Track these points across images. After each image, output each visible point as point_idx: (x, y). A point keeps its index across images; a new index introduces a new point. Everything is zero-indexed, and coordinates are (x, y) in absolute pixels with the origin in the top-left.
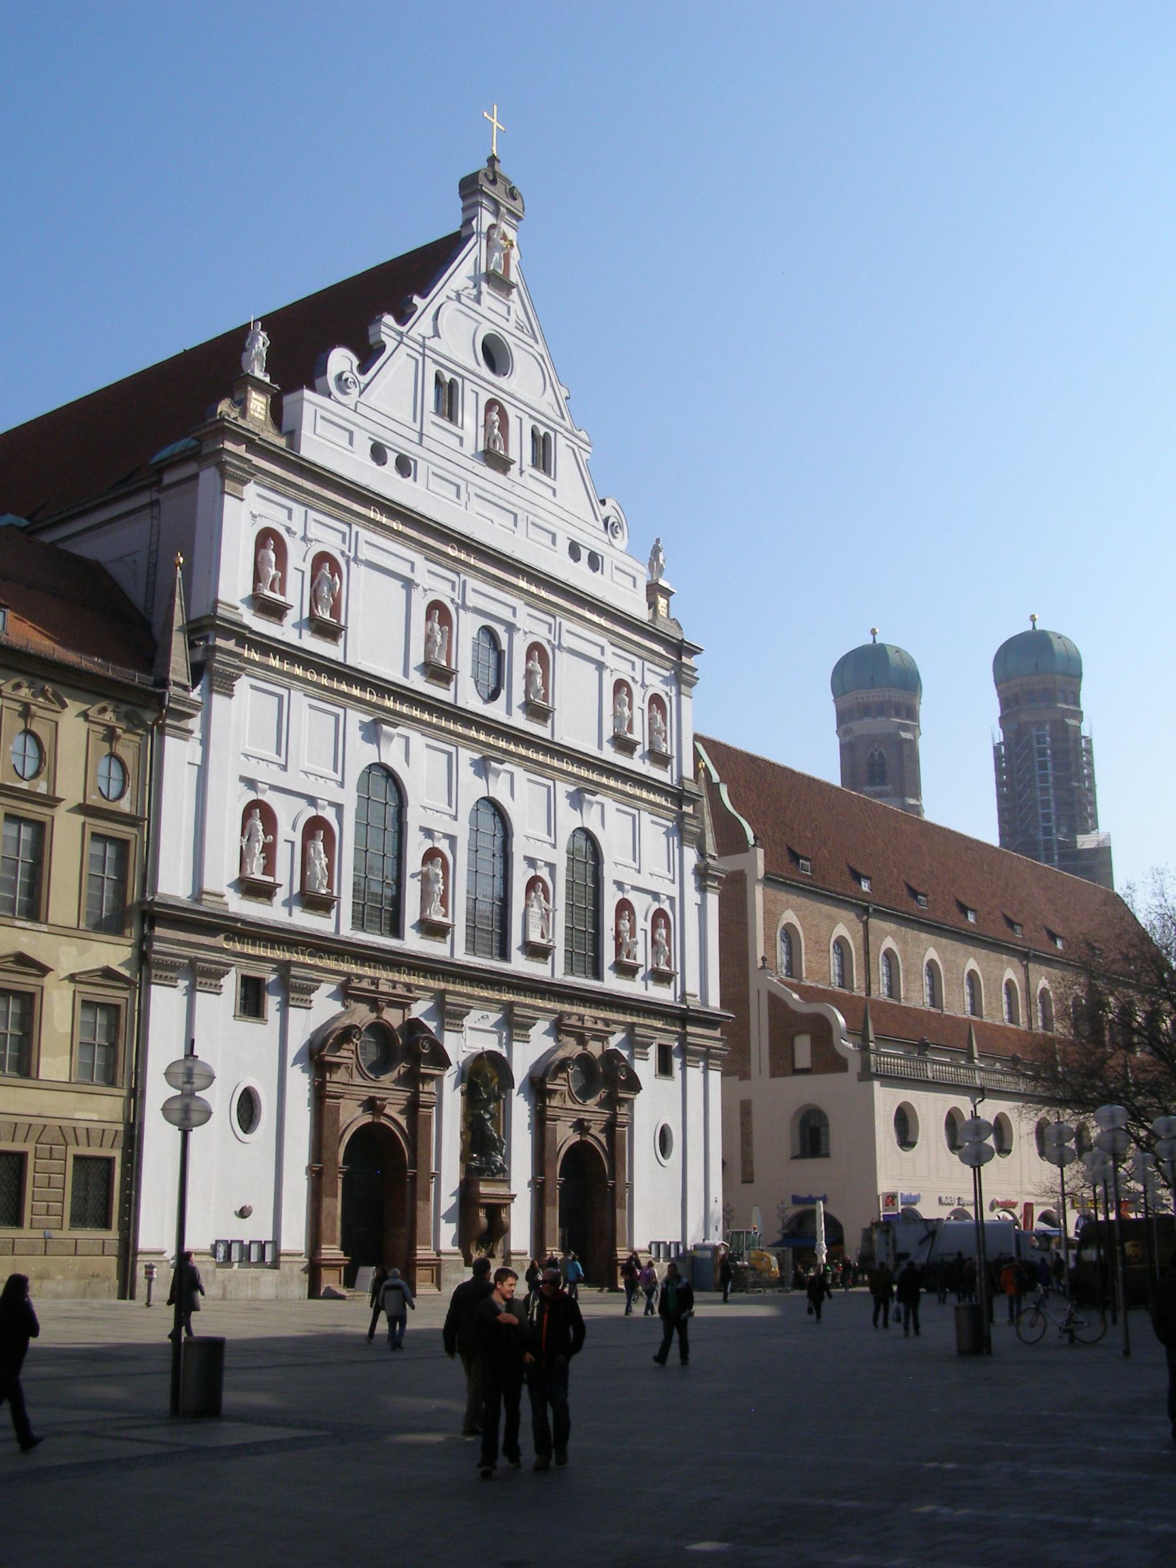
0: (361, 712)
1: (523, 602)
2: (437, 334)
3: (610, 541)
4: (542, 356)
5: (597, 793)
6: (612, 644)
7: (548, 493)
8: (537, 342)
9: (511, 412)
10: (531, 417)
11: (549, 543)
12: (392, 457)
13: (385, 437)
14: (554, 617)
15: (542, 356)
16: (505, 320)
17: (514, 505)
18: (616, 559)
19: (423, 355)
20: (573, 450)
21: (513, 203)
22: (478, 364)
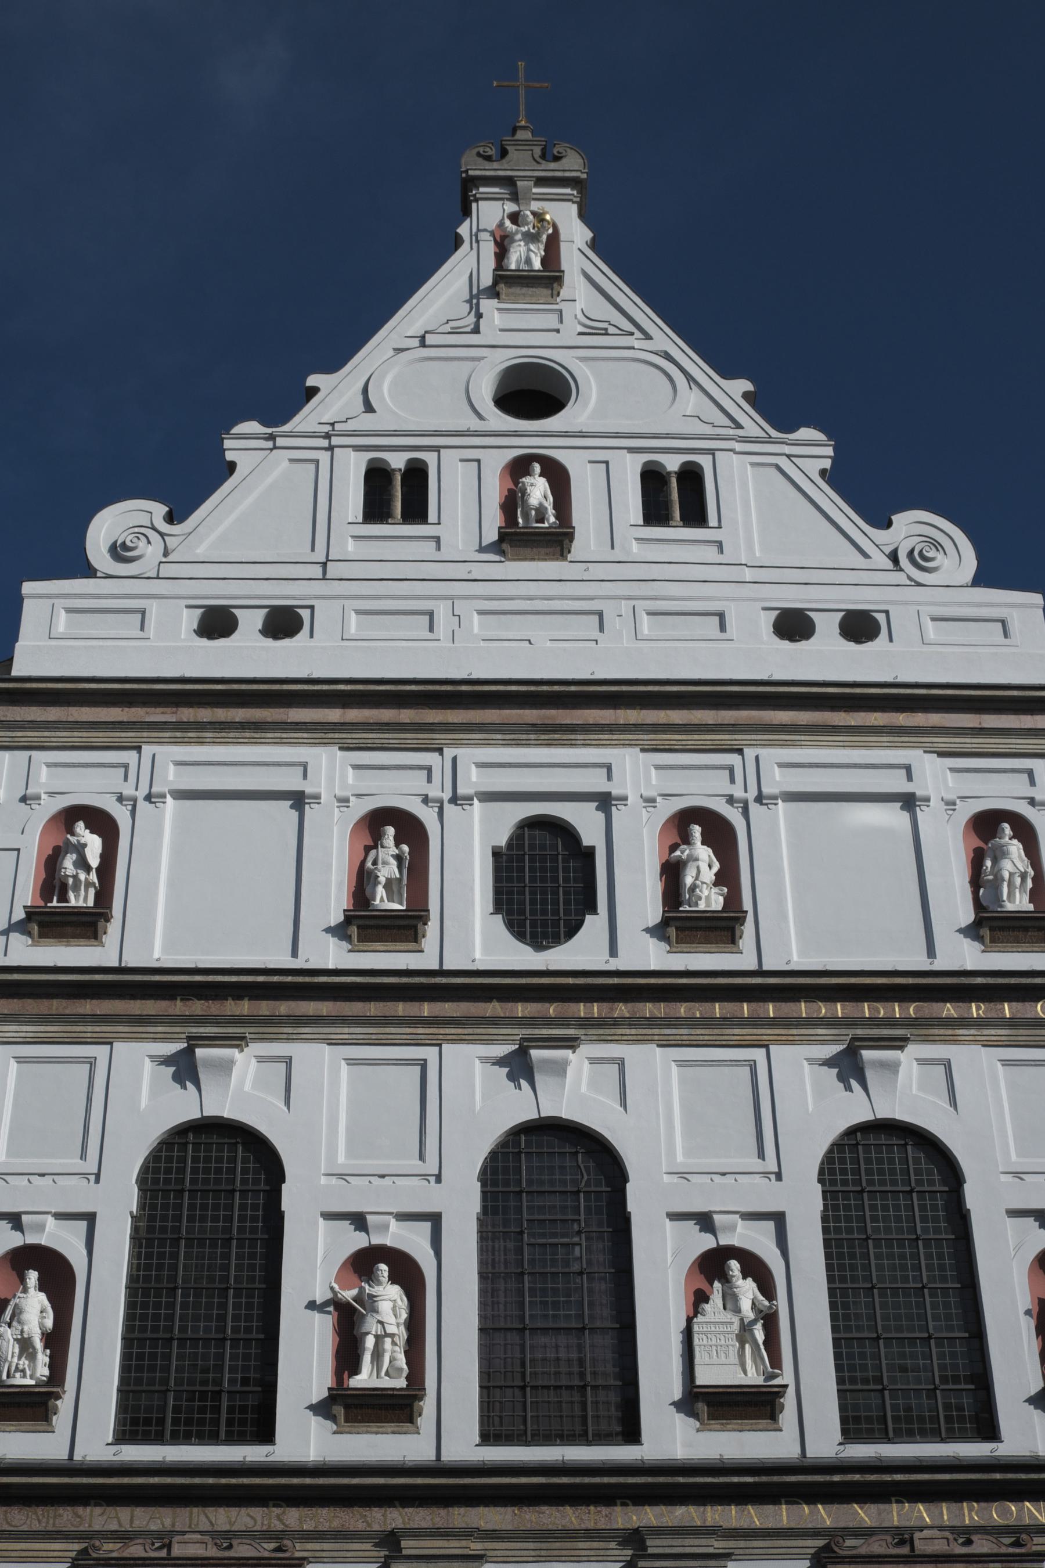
0: (155, 1040)
1: (638, 749)
2: (369, 408)
3: (909, 578)
4: (668, 357)
5: (905, 1040)
6: (941, 754)
7: (710, 554)
8: (648, 337)
9: (572, 461)
10: (631, 450)
11: (716, 633)
12: (250, 622)
13: (219, 594)
14: (740, 751)
15: (668, 357)
16: (555, 333)
17: (592, 598)
18: (919, 603)
19: (331, 448)
20: (778, 468)
21: (553, 165)
22: (481, 417)
